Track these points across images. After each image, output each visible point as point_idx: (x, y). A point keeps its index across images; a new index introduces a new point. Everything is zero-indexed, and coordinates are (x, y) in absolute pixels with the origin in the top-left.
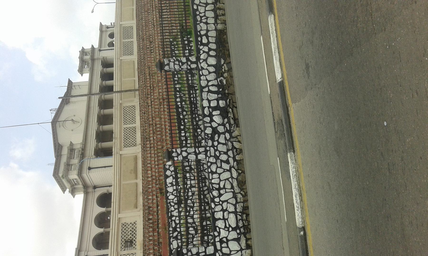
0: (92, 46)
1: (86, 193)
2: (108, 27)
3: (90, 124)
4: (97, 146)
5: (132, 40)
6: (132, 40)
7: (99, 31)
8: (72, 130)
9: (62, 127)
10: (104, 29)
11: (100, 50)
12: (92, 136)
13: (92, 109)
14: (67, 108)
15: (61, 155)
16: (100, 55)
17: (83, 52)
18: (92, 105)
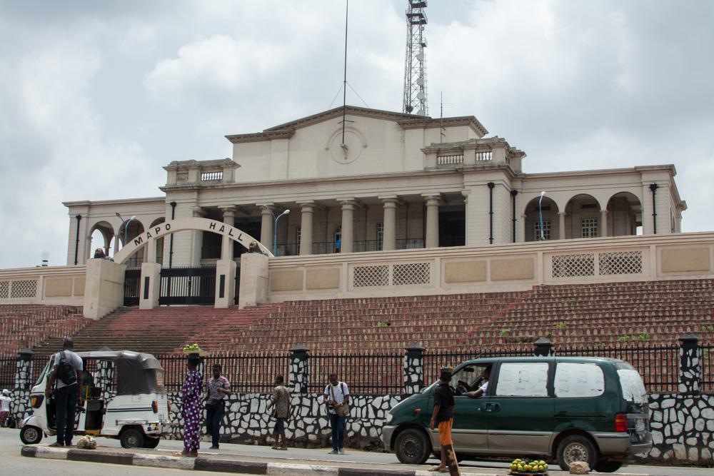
2: (654, 188)
3: (267, 192)
5: (9, 295)
6: (9, 295)
8: (327, 149)
10: (648, 179)
11: (491, 186)
12: (245, 199)
13: (312, 189)
14: (391, 125)
15: (270, 140)
16: (472, 188)
18: (321, 188)
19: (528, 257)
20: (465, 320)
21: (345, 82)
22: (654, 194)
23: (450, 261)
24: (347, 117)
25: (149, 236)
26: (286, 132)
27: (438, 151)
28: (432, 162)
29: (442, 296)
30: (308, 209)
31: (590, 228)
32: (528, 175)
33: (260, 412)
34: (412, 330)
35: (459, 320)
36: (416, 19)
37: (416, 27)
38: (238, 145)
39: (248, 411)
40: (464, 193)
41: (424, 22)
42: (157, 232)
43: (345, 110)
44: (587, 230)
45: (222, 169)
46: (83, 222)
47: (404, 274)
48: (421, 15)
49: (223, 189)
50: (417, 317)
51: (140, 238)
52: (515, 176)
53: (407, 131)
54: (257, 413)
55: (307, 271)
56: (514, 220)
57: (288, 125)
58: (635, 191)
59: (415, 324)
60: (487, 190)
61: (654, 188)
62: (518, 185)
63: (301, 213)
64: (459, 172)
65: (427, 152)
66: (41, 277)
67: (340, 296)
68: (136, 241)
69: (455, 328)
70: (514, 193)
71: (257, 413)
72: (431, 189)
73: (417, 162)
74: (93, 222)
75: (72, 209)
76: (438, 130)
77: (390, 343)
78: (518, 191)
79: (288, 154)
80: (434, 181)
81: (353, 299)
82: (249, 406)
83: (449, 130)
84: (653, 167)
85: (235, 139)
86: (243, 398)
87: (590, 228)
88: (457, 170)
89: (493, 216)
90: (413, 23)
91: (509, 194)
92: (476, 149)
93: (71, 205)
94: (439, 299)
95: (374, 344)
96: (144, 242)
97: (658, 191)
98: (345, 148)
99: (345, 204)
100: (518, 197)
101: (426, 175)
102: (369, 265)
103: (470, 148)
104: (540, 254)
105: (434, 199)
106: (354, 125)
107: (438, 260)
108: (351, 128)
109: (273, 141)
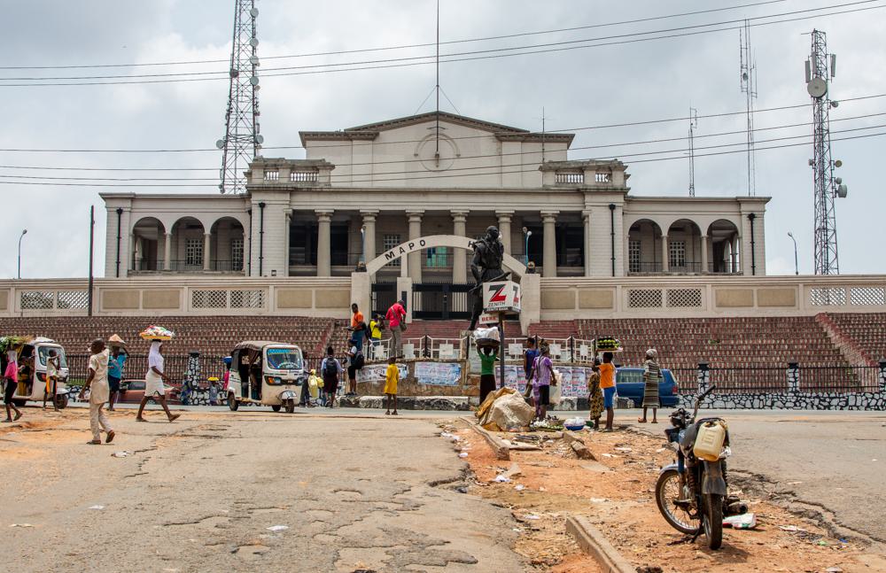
0: (629, 189)
1: (245, 198)
2: (751, 217)
3: (372, 198)
4: (321, 215)
5: (228, 304)
6: (228, 304)
7: (735, 196)
9: (429, 132)
10: (746, 208)
11: (612, 207)
12: (345, 204)
13: (422, 198)
17: (612, 167)
18: (432, 198)
19: (790, 287)
20: (785, 340)
21: (438, 86)
22: (752, 224)
23: (719, 288)
24: (442, 124)
25: (402, 251)
26: (369, 133)
27: (559, 168)
28: (551, 180)
29: (728, 319)
30: (418, 219)
31: (677, 250)
32: (636, 198)
33: (858, 404)
34: (749, 347)
35: (780, 340)
39: (847, 404)
40: (585, 213)
42: (411, 247)
43: (438, 116)
44: (675, 252)
45: (318, 170)
46: (125, 216)
47: (678, 298)
49: (321, 192)
50: (734, 336)
51: (391, 252)
53: (503, 143)
54: (855, 405)
55: (580, 292)
57: (373, 126)
58: (734, 219)
59: (760, 342)
60: (608, 212)
63: (409, 223)
66: (271, 287)
67: (615, 316)
68: (387, 255)
69: (786, 347)
71: (855, 405)
72: (551, 207)
73: (535, 180)
74: (137, 217)
75: (108, 201)
76: (537, 146)
77: (752, 357)
80: (553, 199)
81: (644, 319)
82: (847, 401)
83: (548, 146)
85: (306, 137)
86: (841, 396)
87: (677, 250)
88: (578, 190)
89: (615, 236)
93: (107, 197)
94: (726, 321)
95: (737, 358)
96: (396, 257)
98: (437, 156)
99: (459, 216)
101: (546, 192)
102: (643, 289)
103: (591, 169)
104: (801, 285)
107: (709, 287)
108: (444, 135)
109: (355, 142)
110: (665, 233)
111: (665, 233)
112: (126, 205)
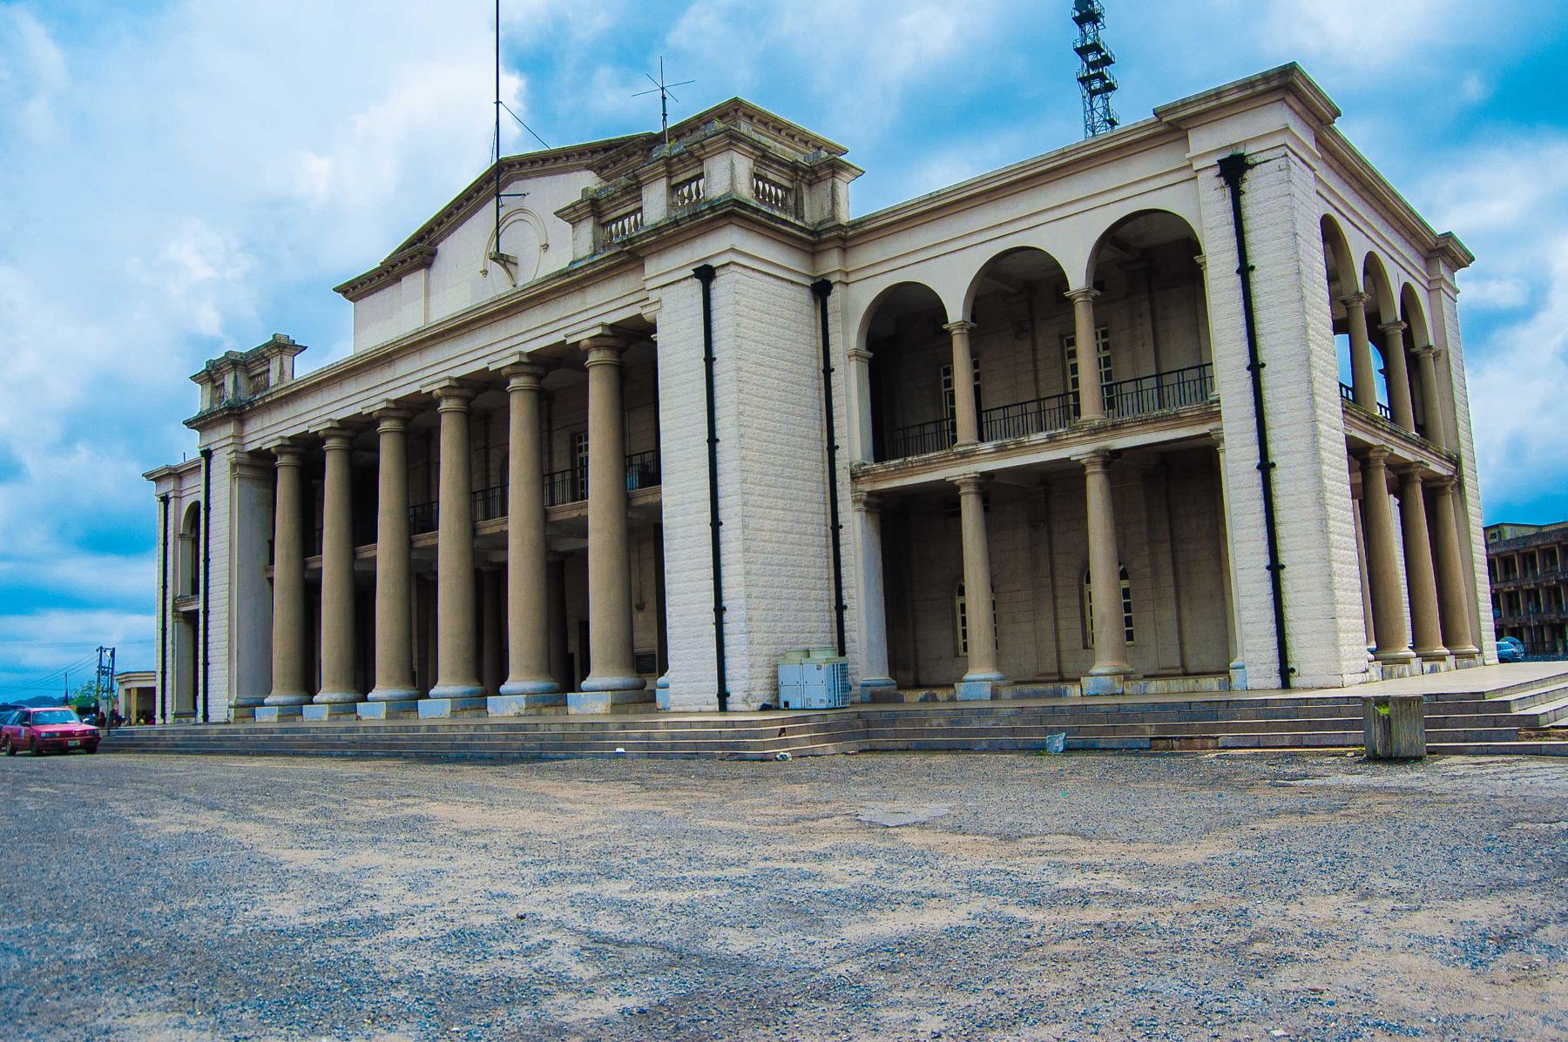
2: (1234, 169)
10: (1208, 142)
11: (706, 275)
15: (398, 279)
18: (403, 367)
21: (498, 103)
22: (1236, 196)
26: (419, 253)
36: (1097, 85)
37: (1098, 101)
38: (366, 302)
40: (647, 313)
41: (1110, 88)
48: (1102, 77)
52: (822, 243)
56: (828, 371)
61: (1234, 169)
62: (831, 263)
64: (627, 257)
65: (571, 215)
70: (821, 290)
72: (580, 319)
78: (833, 279)
79: (427, 302)
84: (1218, 93)
90: (1093, 93)
91: (805, 296)
92: (670, 178)
97: (1256, 185)
100: (835, 299)
105: (598, 348)
106: (527, 203)
110: (956, 312)
111: (956, 312)
112: (169, 487)
